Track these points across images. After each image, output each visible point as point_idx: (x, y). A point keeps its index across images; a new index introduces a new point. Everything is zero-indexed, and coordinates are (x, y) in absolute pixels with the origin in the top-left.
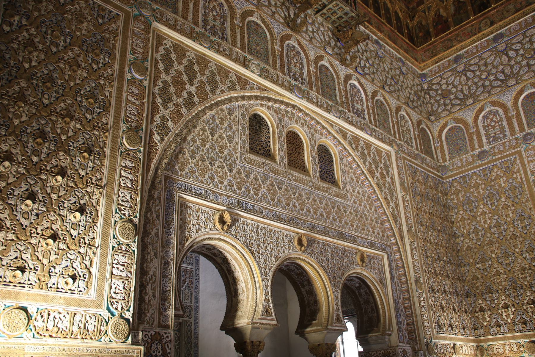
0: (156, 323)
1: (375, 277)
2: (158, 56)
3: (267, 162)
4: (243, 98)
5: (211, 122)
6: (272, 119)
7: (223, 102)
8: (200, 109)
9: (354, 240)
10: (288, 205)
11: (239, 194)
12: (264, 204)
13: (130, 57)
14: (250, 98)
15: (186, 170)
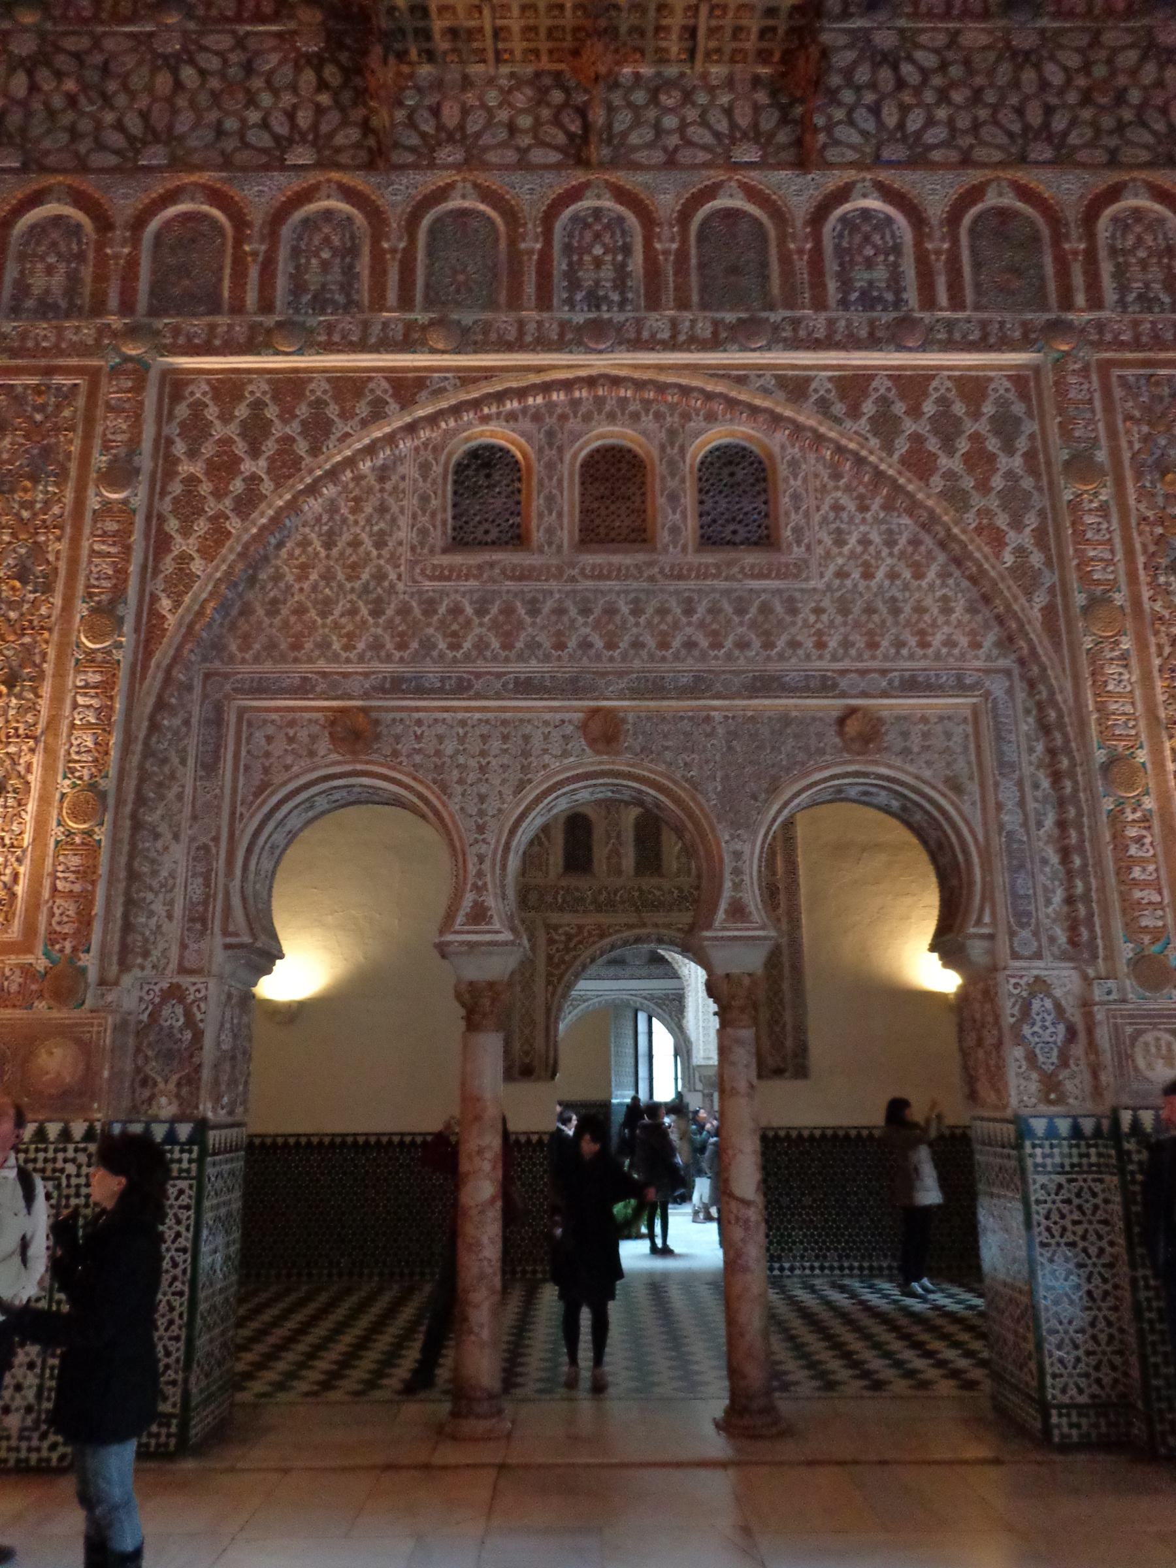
0: (174, 965)
1: (927, 774)
2: (172, 430)
3: (498, 556)
4: (411, 428)
5: (325, 518)
6: (522, 441)
7: (350, 462)
8: (280, 503)
9: (826, 686)
10: (561, 646)
11: (402, 660)
12: (481, 666)
13: (100, 460)
14: (432, 420)
15: (257, 646)
